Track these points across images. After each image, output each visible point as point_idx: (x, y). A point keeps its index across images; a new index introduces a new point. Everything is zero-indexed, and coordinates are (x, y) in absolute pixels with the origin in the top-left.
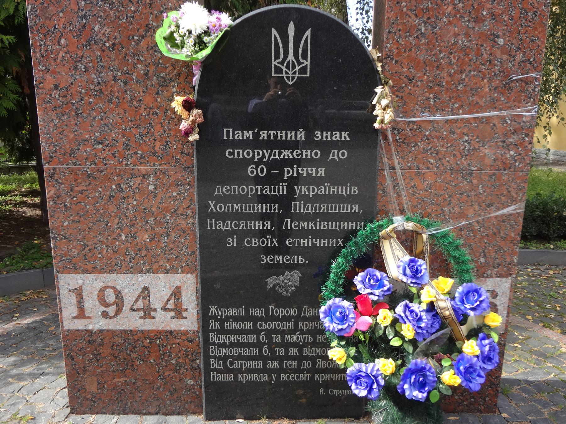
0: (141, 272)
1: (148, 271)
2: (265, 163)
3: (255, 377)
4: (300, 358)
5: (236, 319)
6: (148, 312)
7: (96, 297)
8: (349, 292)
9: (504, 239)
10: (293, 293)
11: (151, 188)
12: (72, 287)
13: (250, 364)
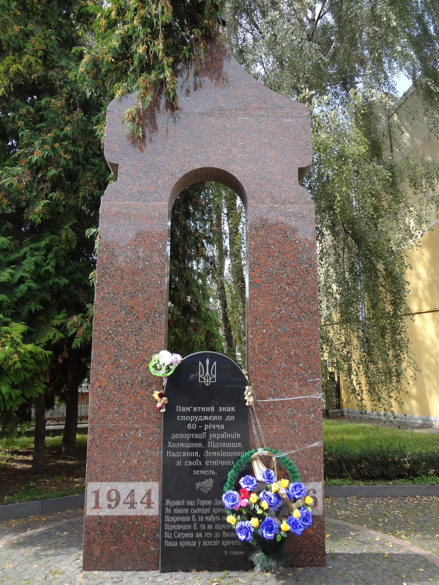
0: (131, 481)
1: (135, 480)
2: (195, 423)
3: (188, 544)
4: (214, 531)
5: (180, 507)
6: (132, 505)
7: (106, 496)
8: (238, 488)
9: (315, 460)
10: (209, 492)
11: (140, 435)
12: (94, 490)
13: (186, 535)
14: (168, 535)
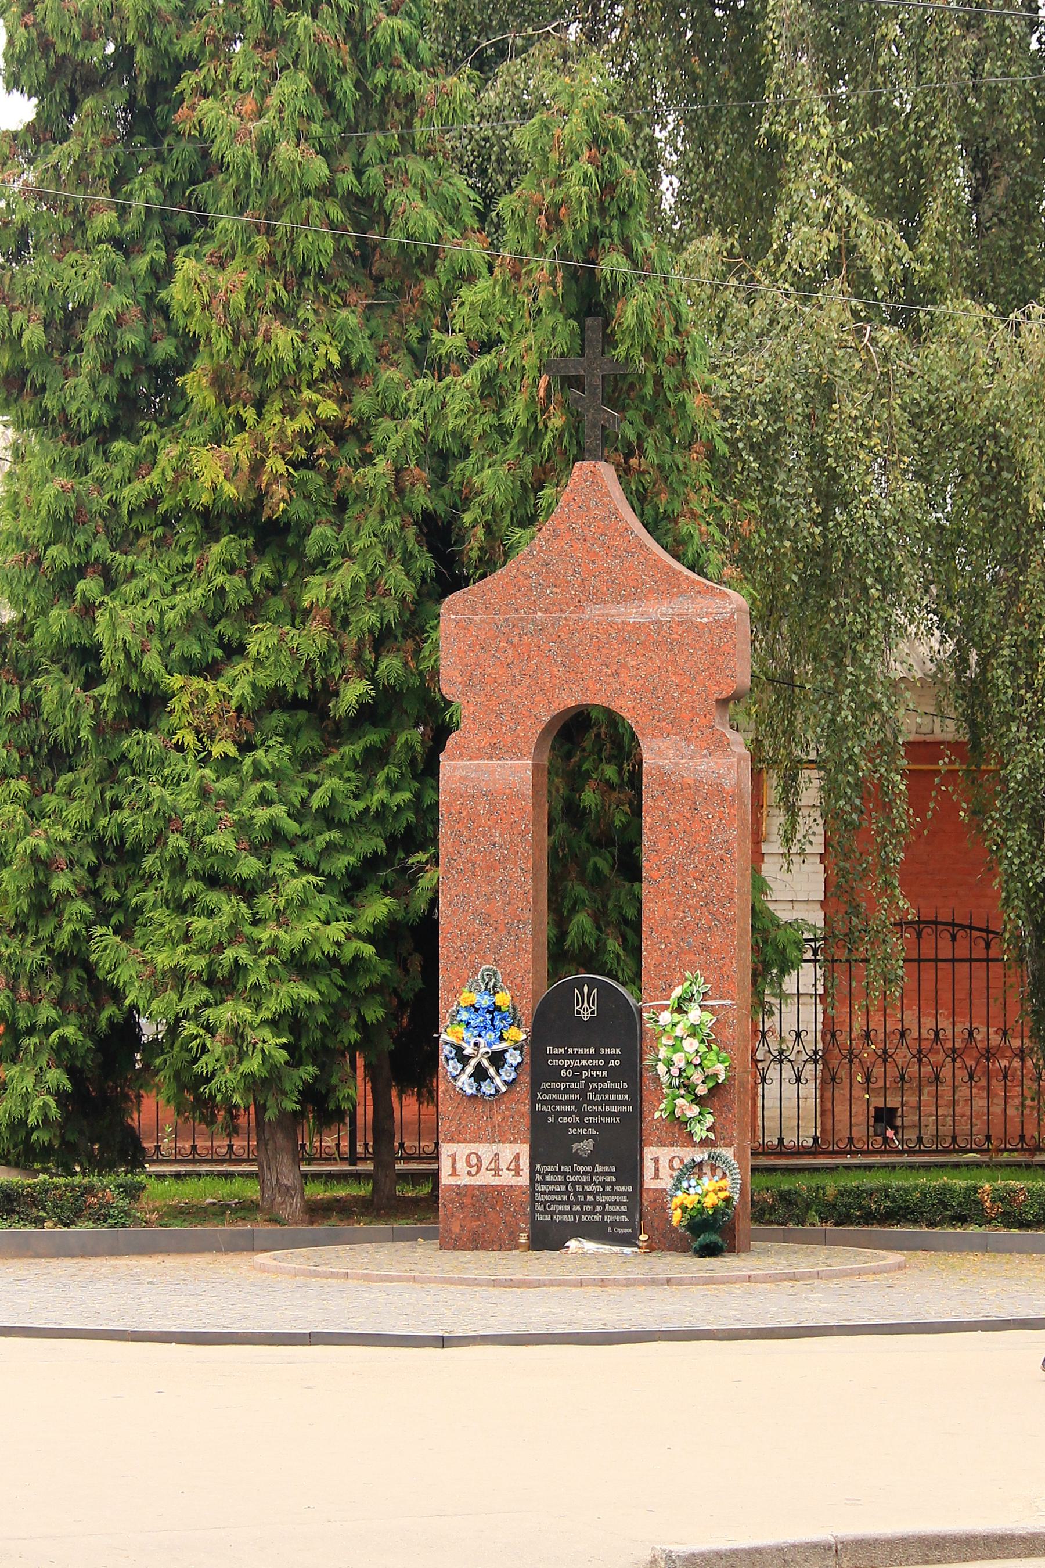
3: (564, 1218)
5: (553, 1173)
6: (497, 1172)
13: (561, 1208)
14: (539, 1207)
